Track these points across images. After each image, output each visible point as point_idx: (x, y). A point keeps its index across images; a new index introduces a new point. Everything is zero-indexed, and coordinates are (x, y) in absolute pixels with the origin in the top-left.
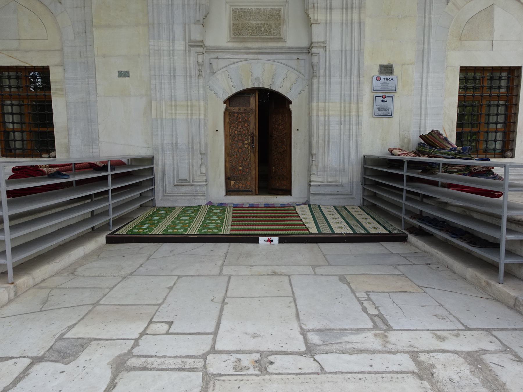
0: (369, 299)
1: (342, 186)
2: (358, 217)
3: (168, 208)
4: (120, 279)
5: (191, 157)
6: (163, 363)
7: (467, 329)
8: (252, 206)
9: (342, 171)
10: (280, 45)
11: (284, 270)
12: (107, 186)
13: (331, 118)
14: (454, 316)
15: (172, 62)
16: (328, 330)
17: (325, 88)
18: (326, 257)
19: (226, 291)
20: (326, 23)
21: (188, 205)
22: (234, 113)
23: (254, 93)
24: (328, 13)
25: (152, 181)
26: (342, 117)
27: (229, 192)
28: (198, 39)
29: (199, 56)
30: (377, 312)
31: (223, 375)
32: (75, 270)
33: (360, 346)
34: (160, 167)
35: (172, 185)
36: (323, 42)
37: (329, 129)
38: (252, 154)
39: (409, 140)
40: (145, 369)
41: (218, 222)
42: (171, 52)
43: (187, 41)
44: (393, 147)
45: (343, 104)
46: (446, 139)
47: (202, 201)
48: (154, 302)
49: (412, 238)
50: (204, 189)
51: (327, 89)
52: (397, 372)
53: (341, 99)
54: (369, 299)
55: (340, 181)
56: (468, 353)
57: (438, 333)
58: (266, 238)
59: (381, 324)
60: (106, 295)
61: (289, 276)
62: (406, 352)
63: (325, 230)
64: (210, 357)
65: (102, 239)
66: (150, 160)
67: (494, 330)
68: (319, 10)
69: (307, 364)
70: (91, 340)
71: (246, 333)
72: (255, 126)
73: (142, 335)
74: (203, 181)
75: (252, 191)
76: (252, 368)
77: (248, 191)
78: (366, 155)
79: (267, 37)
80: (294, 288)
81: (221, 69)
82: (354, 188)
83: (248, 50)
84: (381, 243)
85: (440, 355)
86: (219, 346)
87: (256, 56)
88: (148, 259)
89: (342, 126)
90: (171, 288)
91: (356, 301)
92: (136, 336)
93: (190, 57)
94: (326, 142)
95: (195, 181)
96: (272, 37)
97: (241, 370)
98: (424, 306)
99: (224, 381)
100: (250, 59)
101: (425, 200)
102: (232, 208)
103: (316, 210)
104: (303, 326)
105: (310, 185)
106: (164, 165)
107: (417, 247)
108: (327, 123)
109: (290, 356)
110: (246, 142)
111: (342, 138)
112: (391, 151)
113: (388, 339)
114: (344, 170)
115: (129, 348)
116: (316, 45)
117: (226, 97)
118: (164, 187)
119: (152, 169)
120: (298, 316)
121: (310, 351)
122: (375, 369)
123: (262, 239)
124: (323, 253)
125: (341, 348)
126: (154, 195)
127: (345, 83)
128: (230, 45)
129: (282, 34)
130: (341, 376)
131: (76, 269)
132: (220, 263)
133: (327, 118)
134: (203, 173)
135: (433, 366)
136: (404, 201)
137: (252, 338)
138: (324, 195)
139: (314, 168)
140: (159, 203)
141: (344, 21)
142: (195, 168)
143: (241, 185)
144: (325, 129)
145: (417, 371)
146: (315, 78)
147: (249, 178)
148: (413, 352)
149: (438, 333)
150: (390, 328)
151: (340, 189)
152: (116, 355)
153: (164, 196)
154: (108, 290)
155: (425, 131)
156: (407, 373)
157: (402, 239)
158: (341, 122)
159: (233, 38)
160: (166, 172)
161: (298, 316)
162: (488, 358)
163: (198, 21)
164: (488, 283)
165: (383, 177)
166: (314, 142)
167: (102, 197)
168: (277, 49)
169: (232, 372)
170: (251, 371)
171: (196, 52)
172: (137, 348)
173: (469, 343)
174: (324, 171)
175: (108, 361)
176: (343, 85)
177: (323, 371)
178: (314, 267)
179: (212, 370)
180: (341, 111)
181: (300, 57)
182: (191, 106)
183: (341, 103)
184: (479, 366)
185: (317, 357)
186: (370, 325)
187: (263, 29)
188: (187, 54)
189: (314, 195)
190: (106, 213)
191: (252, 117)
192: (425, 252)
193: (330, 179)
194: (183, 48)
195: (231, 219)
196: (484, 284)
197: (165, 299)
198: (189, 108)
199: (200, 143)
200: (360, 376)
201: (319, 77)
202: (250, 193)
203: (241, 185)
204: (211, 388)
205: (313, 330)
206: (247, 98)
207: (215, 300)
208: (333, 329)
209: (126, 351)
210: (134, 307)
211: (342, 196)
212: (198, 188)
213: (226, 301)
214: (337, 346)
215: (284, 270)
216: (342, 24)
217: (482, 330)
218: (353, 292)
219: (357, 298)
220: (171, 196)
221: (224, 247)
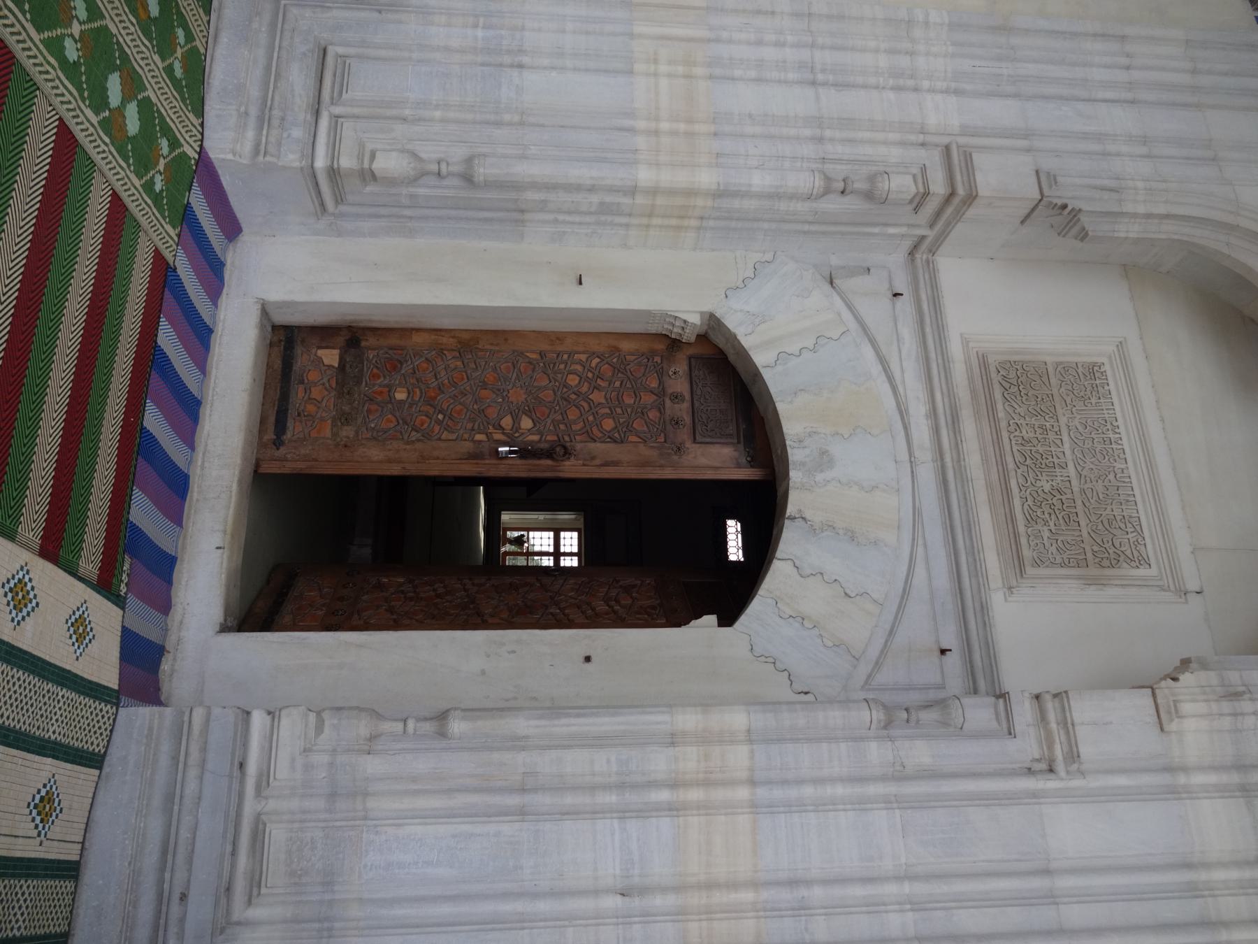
10: (992, 562)
13: (665, 823)
15: (872, 80)
17: (832, 780)
20: (1169, 769)
22: (661, 374)
23: (753, 463)
24: (1224, 778)
26: (671, 900)
27: (286, 341)
28: (979, 178)
29: (909, 179)
36: (1073, 756)
37: (596, 813)
38: (467, 446)
42: (910, 83)
43: (962, 140)
45: (747, 896)
51: (829, 791)
53: (778, 884)
55: (256, 913)
68: (1227, 722)
72: (602, 465)
75: (278, 443)
77: (281, 427)
79: (1017, 502)
81: (850, 307)
83: (945, 421)
87: (925, 455)
89: (619, 898)
93: (902, 144)
94: (513, 800)
96: (1022, 529)
100: (906, 428)
108: (632, 798)
110: (526, 423)
111: (543, 906)
116: (1052, 716)
117: (731, 323)
127: (874, 906)
128: (955, 349)
129: (1042, 571)
133: (664, 796)
134: (373, 156)
141: (1203, 876)
144: (593, 789)
146: (878, 715)
147: (347, 432)
151: (199, 910)
158: (644, 891)
159: (983, 361)
163: (1053, 179)
166: (522, 725)
168: (974, 552)
171: (924, 169)
176: (859, 891)
180: (710, 886)
181: (953, 660)
182: (690, 135)
183: (755, 885)
187: (1047, 487)
188: (913, 138)
191: (646, 452)
193: (277, 835)
194: (932, 121)
198: (682, 127)
199: (523, 157)
201: (891, 739)
202: (270, 435)
203: (316, 393)
206: (732, 429)
212: (297, 133)
216: (1189, 866)
220: (273, 25)
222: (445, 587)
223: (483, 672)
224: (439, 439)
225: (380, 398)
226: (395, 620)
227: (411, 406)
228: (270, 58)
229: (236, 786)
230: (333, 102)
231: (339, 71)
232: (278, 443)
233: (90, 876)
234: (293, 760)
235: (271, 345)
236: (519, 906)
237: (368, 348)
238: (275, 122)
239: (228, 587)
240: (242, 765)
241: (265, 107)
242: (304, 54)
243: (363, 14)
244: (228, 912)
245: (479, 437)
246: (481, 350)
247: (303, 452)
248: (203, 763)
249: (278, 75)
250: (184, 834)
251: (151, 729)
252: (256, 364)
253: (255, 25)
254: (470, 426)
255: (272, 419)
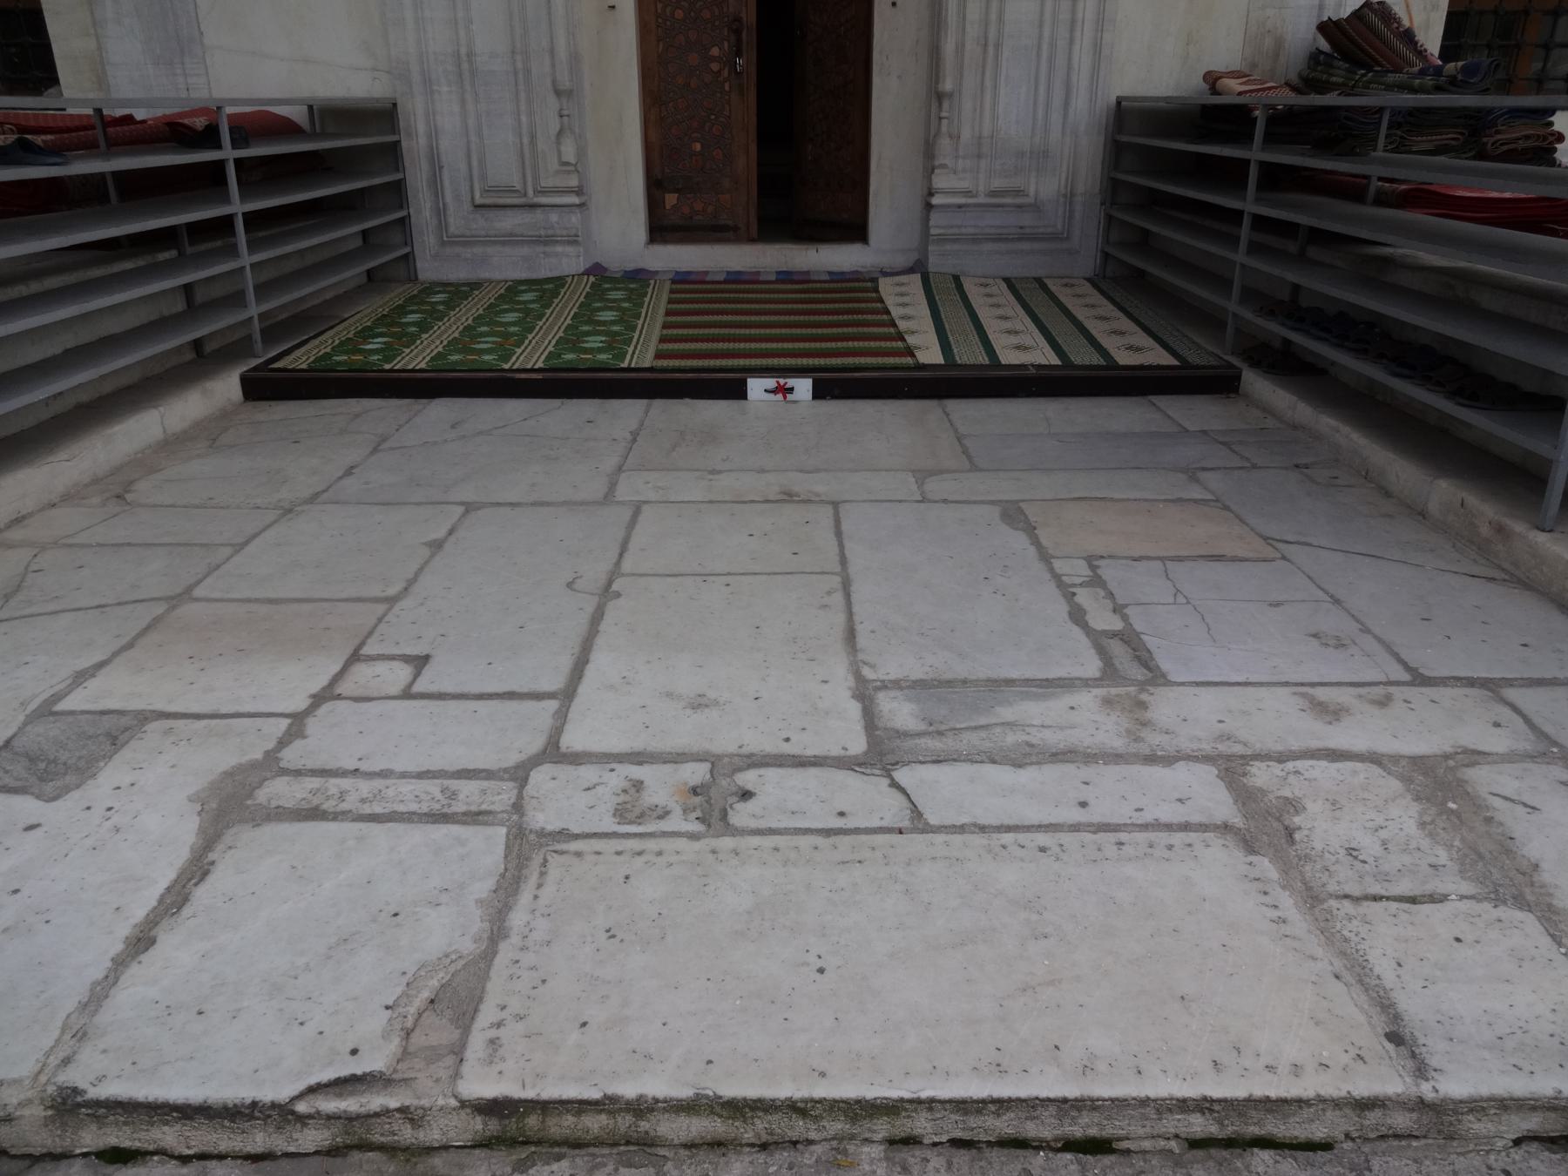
0: (1096, 581)
1: (1036, 207)
2: (1080, 314)
3: (457, 285)
4: (271, 516)
5: (523, 107)
6: (377, 796)
7: (1420, 679)
8: (734, 278)
11: (820, 485)
12: (226, 200)
14: (1376, 637)
16: (949, 683)
18: (966, 442)
19: (621, 555)
21: (524, 275)
25: (397, 192)
27: (660, 230)
30: (1117, 624)
31: (577, 837)
32: (128, 486)
33: (1053, 739)
34: (422, 141)
35: (467, 206)
39: (1279, 43)
40: (314, 814)
41: (615, 328)
44: (1219, 65)
46: (1408, 36)
47: (568, 262)
48: (376, 591)
49: (1256, 383)
50: (575, 219)
52: (1169, 827)
54: (1096, 581)
56: (1416, 761)
57: (1321, 694)
58: (771, 383)
59: (1130, 665)
60: (218, 567)
61: (836, 505)
62: (1207, 759)
63: (969, 354)
64: (540, 777)
65: (227, 386)
66: (385, 115)
67: (1510, 683)
69: (868, 798)
70: (144, 718)
71: (669, 695)
73: (319, 699)
74: (568, 191)
75: (735, 229)
76: (678, 811)
78: (1127, 98)
80: (848, 544)
84: (1153, 398)
85: (1321, 771)
86: (573, 739)
88: (375, 450)
90: (437, 546)
91: (1051, 588)
92: (299, 703)
94: (991, 50)
95: (543, 192)
97: (641, 818)
98: (1277, 604)
99: (578, 854)
101: (1313, 252)
102: (667, 286)
103: (946, 294)
104: (867, 673)
105: (929, 206)
106: (433, 134)
107: (1267, 410)
109: (813, 771)
110: (715, 51)
112: (1212, 79)
113: (1149, 715)
115: (271, 745)
118: (440, 212)
119: (392, 153)
120: (851, 635)
121: (882, 755)
122: (1095, 815)
123: (757, 387)
124: (956, 431)
125: (988, 744)
126: (408, 240)
130: (977, 840)
131: (132, 482)
132: (611, 462)
134: (567, 164)
135: (1294, 805)
136: (1240, 257)
137: (689, 712)
139: (945, 144)
140: (429, 269)
142: (541, 145)
145: (1237, 821)
148: (1229, 758)
149: (1321, 694)
150: (1157, 678)
151: (1027, 220)
152: (221, 770)
153: (443, 244)
154: (228, 551)
155: (1339, 5)
156: (1203, 828)
157: (1221, 384)
160: (444, 159)
161: (851, 635)
162: (1482, 778)
164: (1500, 529)
165: (1180, 174)
166: (949, 47)
167: (219, 243)
169: (609, 824)
170: (676, 823)
172: (298, 744)
173: (1422, 728)
174: (979, 156)
175: (191, 790)
177: (918, 822)
178: (922, 476)
179: (542, 819)
184: (1452, 805)
185: (901, 775)
186: (1091, 666)
190: (236, 299)
192: (1295, 427)
193: (997, 183)
195: (660, 319)
196: (1485, 531)
197: (411, 583)
199: (552, 52)
200: (1042, 839)
204: (533, 879)
205: (897, 684)
207: (579, 585)
208: (965, 682)
209: (258, 755)
210: (306, 607)
211: (1037, 246)
212: (554, 217)
213: (615, 587)
214: (974, 739)
215: (820, 485)
217: (1471, 682)
218: (1045, 557)
219: (1057, 578)
220: (466, 244)
221: (629, 411)
223: (899, 77)
230: (525, 195)
232: (735, 229)
233: (1008, 275)
236: (1045, 47)
238: (550, 232)
240: (960, 206)
243: (447, 183)
244: (1030, 205)
249: (511, 235)
250: (993, 231)
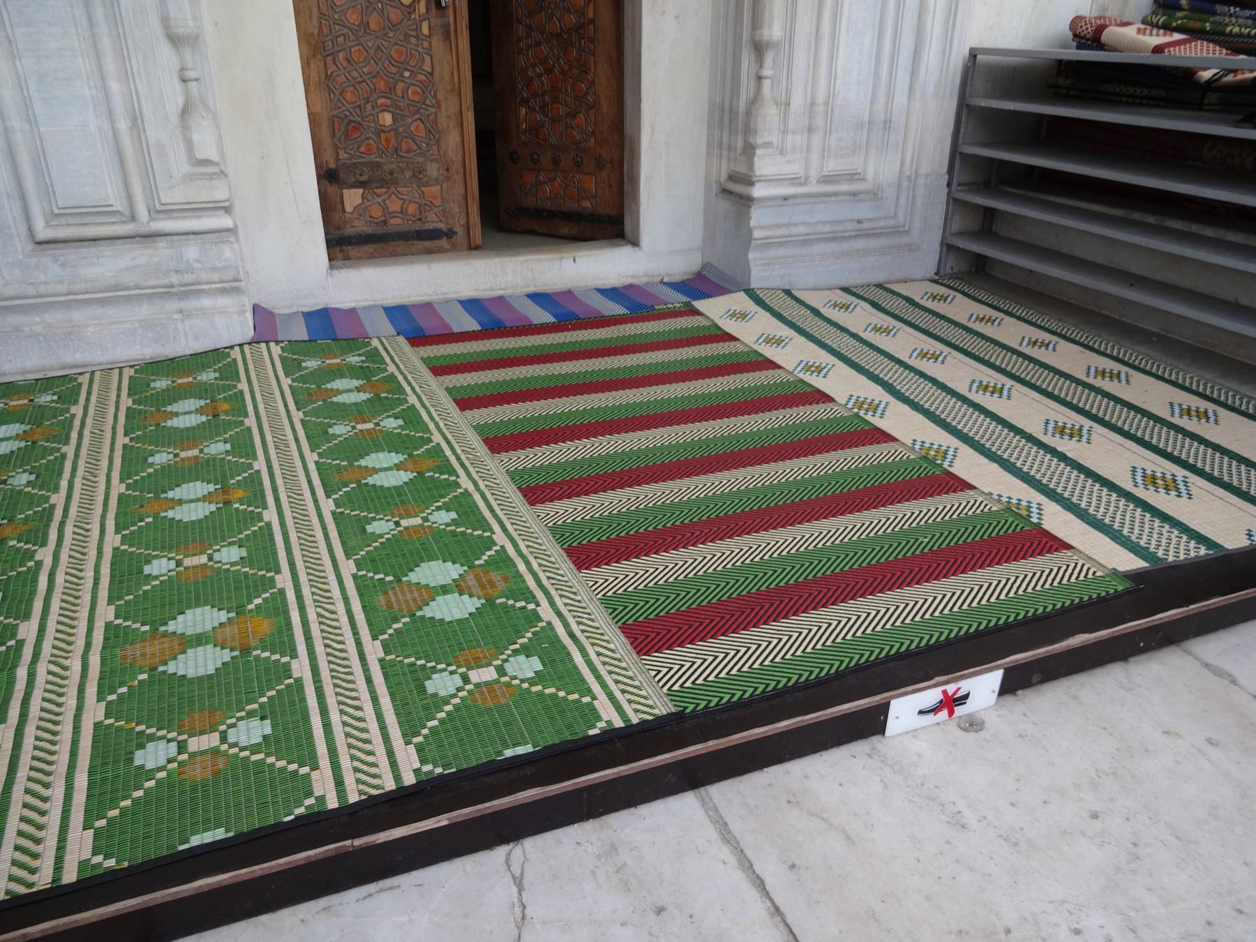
1: (874, 195)
9: (880, 127)
27: (343, 244)
35: (21, 245)
38: (437, 43)
55: (870, 177)
75: (450, 234)
77: (434, 235)
82: (919, 202)
95: (168, 213)
114: (887, 123)
134: (206, 162)
138: (805, 242)
139: (769, 116)
142: (153, 133)
143: (396, 206)
147: (433, 170)
151: (864, 210)
174: (810, 130)
189: (767, 244)
193: (833, 166)
202: (444, 242)
203: (394, 206)
212: (191, 252)
222: (533, 65)
224: (432, 74)
225: (394, 141)
226: (590, 107)
227: (398, 107)
228: (87, 302)
229: (799, 201)
230: (133, 218)
231: (71, 220)
232: (450, 234)
234: (789, 162)
235: (347, 258)
237: (337, 159)
238: (189, 278)
239: (601, 248)
240: (785, 199)
241: (168, 293)
242: (63, 265)
244: (867, 192)
245: (425, 30)
246: (320, 30)
247: (457, 210)
248: (787, 225)
249: (116, 288)
250: (827, 228)
251: (764, 265)
252: (395, 264)
253: (38, 329)
254: (413, 40)
255: (427, 244)
